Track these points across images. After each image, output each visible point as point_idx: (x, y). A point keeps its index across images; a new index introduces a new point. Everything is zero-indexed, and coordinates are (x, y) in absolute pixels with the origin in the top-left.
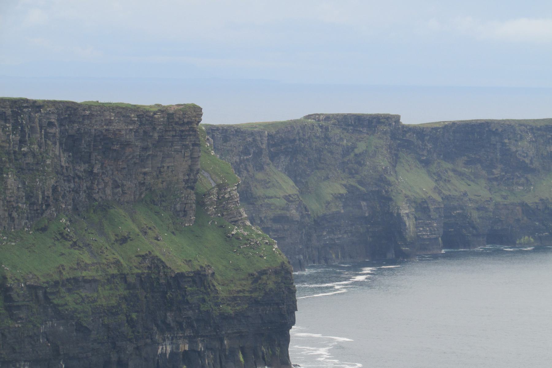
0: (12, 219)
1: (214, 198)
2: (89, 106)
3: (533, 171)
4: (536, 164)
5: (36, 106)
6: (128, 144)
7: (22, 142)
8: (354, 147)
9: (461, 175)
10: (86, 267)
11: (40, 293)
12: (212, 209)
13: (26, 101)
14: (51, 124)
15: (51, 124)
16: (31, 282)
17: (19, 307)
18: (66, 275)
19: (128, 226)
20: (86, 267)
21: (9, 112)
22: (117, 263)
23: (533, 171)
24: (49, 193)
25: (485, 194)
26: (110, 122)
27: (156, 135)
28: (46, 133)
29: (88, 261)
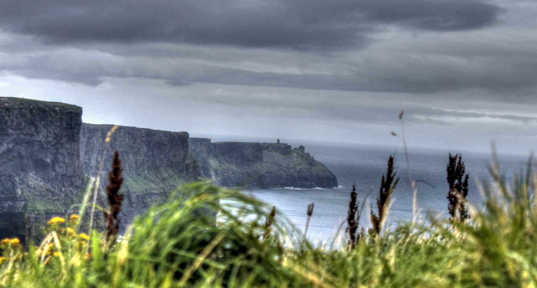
0: (130, 170)
1: (192, 166)
2: (155, 131)
3: (251, 161)
4: (252, 159)
5: (140, 130)
6: (165, 145)
7: (134, 143)
8: (195, 150)
9: (226, 161)
10: (154, 189)
11: (140, 198)
12: (191, 170)
13: (135, 128)
14: (143, 137)
15: (143, 137)
16: (137, 194)
17: (133, 203)
18: (148, 192)
19: (165, 175)
20: (154, 189)
21: (130, 132)
22: (163, 188)
23: (251, 161)
24: (141, 162)
25: (236, 169)
26: (161, 137)
27: (174, 142)
28: (142, 141)
29: (154, 187)
